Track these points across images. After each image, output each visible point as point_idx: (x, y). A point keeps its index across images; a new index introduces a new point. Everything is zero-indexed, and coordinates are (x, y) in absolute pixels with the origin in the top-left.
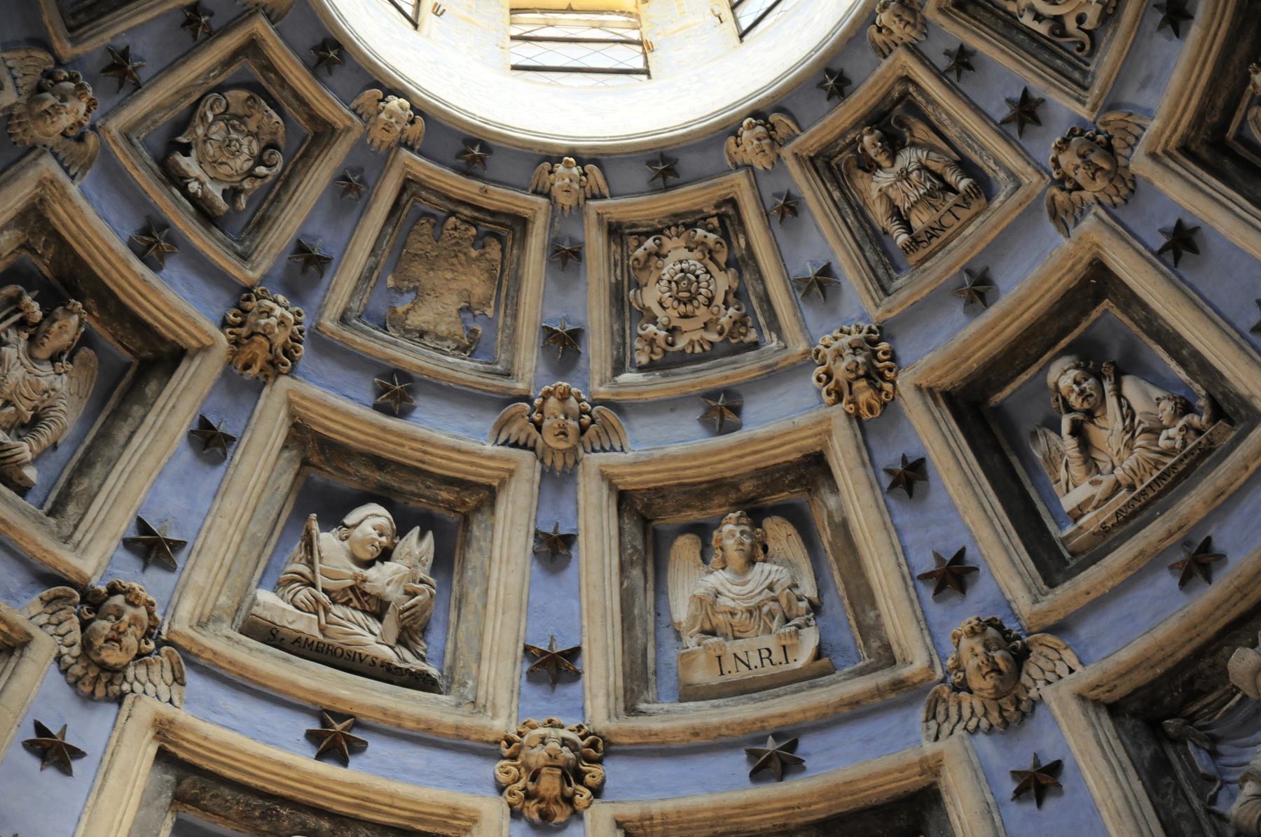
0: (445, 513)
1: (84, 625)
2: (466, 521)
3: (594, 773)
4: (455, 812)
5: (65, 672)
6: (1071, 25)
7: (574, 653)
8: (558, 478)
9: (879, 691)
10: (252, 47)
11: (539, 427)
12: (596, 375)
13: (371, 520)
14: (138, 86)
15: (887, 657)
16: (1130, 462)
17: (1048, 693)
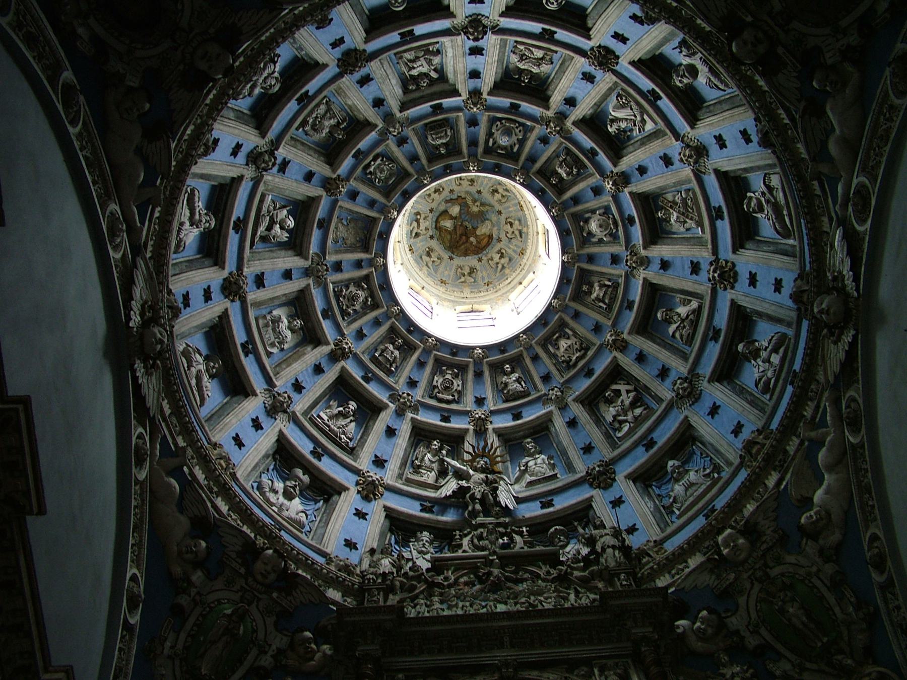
0: (296, 243)
1: (266, 152)
2: (290, 249)
3: (237, 298)
4: (224, 263)
5: (255, 148)
6: (436, 390)
7: (264, 287)
8: (307, 272)
9: (268, 374)
10: (407, 175)
11: (318, 264)
12: (332, 278)
13: (291, 223)
14: (399, 146)
15: (276, 374)
16: (336, 429)
17: (278, 421)
